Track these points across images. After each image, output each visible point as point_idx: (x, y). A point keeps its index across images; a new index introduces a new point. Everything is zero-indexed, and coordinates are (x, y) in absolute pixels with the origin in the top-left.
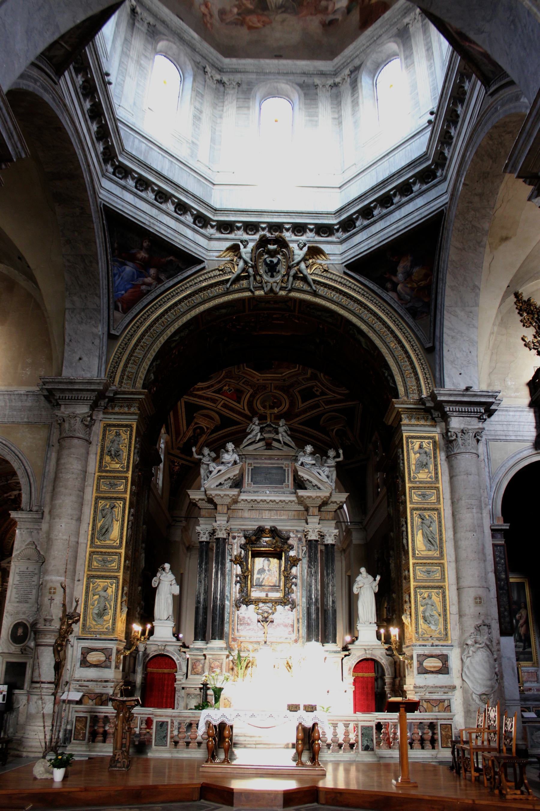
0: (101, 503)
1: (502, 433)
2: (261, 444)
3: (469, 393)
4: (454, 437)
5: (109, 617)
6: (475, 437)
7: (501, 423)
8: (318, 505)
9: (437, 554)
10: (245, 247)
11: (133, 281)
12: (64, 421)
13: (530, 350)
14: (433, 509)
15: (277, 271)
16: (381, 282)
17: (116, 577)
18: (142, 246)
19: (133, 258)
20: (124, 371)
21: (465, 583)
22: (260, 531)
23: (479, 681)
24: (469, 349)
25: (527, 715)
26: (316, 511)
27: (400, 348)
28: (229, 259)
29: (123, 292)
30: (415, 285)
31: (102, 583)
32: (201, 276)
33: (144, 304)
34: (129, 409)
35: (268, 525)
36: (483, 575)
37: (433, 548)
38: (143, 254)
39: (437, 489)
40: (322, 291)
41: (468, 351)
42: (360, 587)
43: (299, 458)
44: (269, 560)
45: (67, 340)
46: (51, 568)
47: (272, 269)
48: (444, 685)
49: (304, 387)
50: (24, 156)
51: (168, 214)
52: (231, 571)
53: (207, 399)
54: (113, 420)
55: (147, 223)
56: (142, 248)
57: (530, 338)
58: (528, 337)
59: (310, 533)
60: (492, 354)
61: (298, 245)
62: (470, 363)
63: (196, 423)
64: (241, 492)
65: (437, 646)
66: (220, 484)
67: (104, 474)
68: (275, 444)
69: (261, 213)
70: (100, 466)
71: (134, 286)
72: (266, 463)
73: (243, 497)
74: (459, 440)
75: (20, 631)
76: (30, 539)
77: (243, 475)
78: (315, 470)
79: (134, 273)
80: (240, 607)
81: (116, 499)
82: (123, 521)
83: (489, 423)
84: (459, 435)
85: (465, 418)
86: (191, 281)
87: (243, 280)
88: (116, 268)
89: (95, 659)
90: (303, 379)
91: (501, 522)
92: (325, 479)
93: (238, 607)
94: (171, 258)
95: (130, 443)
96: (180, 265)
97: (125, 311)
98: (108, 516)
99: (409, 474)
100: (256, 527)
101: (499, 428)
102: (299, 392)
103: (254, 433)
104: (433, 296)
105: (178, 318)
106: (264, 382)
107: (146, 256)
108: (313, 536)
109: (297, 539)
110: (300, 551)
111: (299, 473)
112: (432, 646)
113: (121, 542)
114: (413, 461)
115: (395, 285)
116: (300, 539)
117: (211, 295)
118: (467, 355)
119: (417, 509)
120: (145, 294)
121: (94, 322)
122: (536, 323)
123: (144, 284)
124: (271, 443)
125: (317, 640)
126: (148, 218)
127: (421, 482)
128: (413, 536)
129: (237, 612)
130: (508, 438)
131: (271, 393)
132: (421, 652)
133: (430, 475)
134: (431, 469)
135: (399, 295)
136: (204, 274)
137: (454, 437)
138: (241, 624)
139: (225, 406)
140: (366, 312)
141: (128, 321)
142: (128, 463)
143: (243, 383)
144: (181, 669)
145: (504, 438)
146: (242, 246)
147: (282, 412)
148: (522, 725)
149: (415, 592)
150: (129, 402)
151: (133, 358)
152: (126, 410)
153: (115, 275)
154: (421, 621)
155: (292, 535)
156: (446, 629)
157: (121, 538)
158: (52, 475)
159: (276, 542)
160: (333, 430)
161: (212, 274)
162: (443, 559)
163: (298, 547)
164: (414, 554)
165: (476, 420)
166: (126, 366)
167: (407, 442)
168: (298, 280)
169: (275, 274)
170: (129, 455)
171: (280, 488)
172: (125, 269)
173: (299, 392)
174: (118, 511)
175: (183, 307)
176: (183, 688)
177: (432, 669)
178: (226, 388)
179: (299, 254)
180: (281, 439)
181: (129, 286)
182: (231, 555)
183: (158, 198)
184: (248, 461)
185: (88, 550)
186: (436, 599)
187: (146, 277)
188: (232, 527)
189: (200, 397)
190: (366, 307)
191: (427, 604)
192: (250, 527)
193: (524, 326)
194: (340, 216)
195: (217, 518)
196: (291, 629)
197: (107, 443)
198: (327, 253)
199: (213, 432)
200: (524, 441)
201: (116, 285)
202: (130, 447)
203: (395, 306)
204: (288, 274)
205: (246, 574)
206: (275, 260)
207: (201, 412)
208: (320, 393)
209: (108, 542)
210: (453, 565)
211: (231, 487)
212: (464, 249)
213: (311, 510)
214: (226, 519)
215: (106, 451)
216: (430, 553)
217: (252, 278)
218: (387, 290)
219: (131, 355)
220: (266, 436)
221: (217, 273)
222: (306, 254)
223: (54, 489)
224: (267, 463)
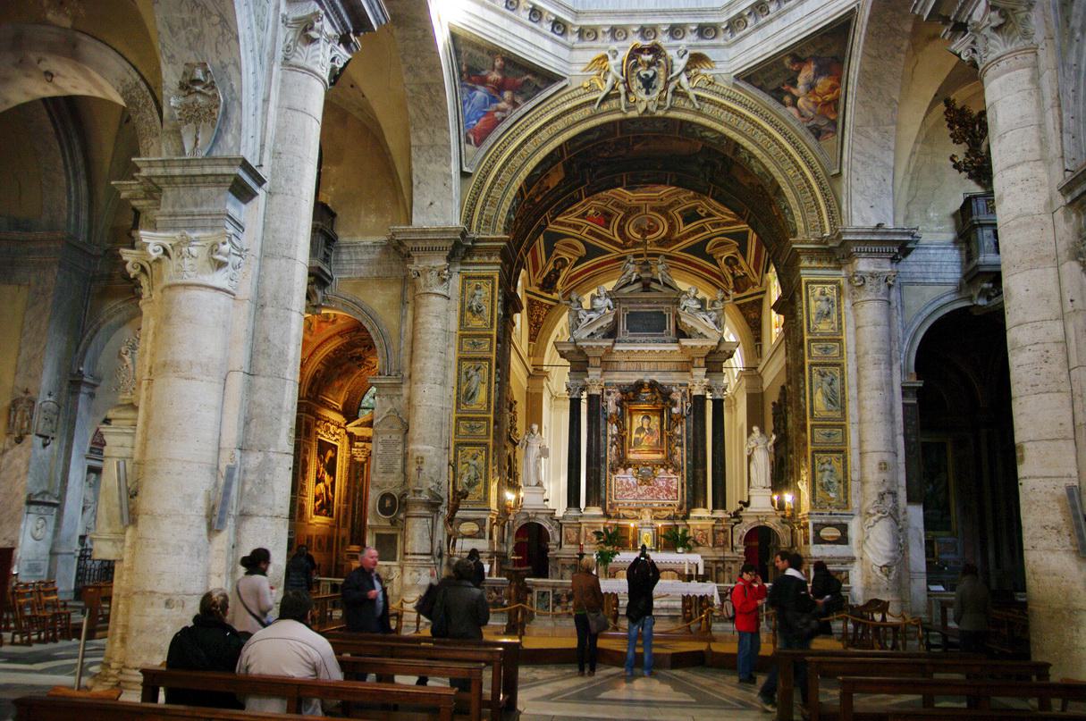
0: (466, 364)
1: (919, 275)
2: (637, 286)
3: (880, 230)
4: (862, 282)
5: (481, 486)
6: (886, 281)
8: (703, 356)
9: (838, 415)
10: (614, 57)
11: (485, 108)
12: (419, 275)
13: (960, 172)
14: (835, 365)
16: (778, 94)
17: (485, 444)
18: (494, 65)
19: (483, 81)
20: (481, 213)
21: (867, 447)
22: (639, 386)
23: (882, 552)
24: (882, 176)
25: (933, 588)
26: (702, 363)
27: (800, 177)
28: (595, 72)
29: (475, 122)
30: (820, 100)
31: (470, 450)
32: (563, 95)
33: (499, 134)
34: (489, 258)
35: (647, 379)
36: (890, 438)
37: (835, 408)
39: (840, 341)
40: (707, 109)
42: (753, 449)
43: (682, 301)
44: (648, 418)
45: (415, 182)
46: (416, 437)
47: (648, 83)
48: (842, 555)
49: (685, 207)
50: (384, 22)
51: (521, 24)
52: (606, 431)
53: (570, 226)
54: (472, 271)
55: (498, 37)
56: (493, 70)
57: (961, 158)
58: (959, 157)
59: (697, 387)
60: (912, 179)
61: (678, 53)
63: (557, 255)
64: (615, 342)
65: (835, 514)
66: (592, 334)
67: (466, 332)
68: (654, 285)
69: (632, 14)
70: (461, 325)
71: (486, 114)
72: (643, 308)
73: (618, 347)
74: (868, 286)
75: (388, 503)
76: (391, 406)
77: (617, 325)
78: (701, 316)
79: (486, 99)
80: (617, 470)
81: (481, 359)
82: (490, 383)
84: (868, 279)
86: (552, 103)
87: (612, 99)
88: (465, 95)
89: (467, 530)
90: (684, 198)
91: (914, 379)
92: (712, 326)
93: (614, 471)
94: (528, 77)
95: (493, 297)
96: (538, 84)
97: (478, 144)
98: (475, 378)
99: (809, 325)
100: (634, 381)
101: (916, 269)
102: (680, 213)
103: (629, 273)
104: (841, 113)
105: (539, 149)
106: (637, 202)
107: (500, 77)
108: (697, 391)
109: (679, 393)
110: (685, 408)
111: (682, 319)
112: (831, 514)
113: (489, 407)
114: (813, 310)
115: (795, 99)
116: (684, 395)
117: (576, 120)
118: (880, 183)
119: (816, 365)
120: (499, 122)
121: (444, 160)
122: (970, 137)
123: (498, 110)
124: (649, 284)
125: (705, 506)
126: (499, 32)
127: (822, 334)
128: (811, 394)
129: (613, 477)
130: (926, 281)
131: (645, 216)
132: (819, 521)
133: (832, 326)
135: (799, 111)
136: (566, 94)
137: (862, 282)
138: (619, 491)
139: (591, 233)
140: (760, 133)
141: (482, 155)
142: (492, 319)
143: (612, 205)
144: (554, 538)
145: (922, 281)
146: (610, 57)
147: (659, 238)
148: (926, 598)
149: (813, 456)
150: (489, 252)
151: (490, 199)
152: (486, 259)
154: (818, 489)
155: (674, 389)
156: (846, 497)
157: (489, 402)
158: (409, 335)
159: (656, 399)
160: (721, 258)
161: (576, 93)
162: (845, 421)
163: (682, 403)
164: (812, 414)
165: (888, 262)
166: (483, 207)
167: (807, 288)
168: (678, 96)
169: (650, 90)
170: (492, 310)
171: (660, 336)
172: (475, 94)
173: (680, 213)
174: (484, 372)
175: (544, 135)
176: (557, 558)
177: (830, 539)
178: (592, 211)
179: (680, 64)
180: (660, 279)
182: (606, 414)
183: (509, 4)
184: (623, 306)
185: (454, 416)
186: (837, 465)
188: (607, 381)
189: (561, 224)
190: (758, 126)
191: (824, 470)
192: (627, 381)
193: (954, 142)
194: (728, 13)
195: (590, 373)
196: (674, 495)
197: (467, 298)
198: (713, 60)
199: (577, 264)
200: (946, 284)
201: (467, 113)
202: (493, 301)
203: (794, 125)
204: (666, 88)
205: (624, 434)
206: (650, 73)
207: (561, 241)
208: (706, 214)
209: (474, 407)
210: (856, 427)
211: (604, 337)
212: (880, 56)
213: (696, 361)
214: (599, 373)
215: (467, 306)
216: (830, 414)
217: (623, 97)
218: (784, 104)
219: (488, 195)
220: (643, 276)
221: (583, 91)
222: (688, 63)
223: (412, 352)
224: (645, 308)
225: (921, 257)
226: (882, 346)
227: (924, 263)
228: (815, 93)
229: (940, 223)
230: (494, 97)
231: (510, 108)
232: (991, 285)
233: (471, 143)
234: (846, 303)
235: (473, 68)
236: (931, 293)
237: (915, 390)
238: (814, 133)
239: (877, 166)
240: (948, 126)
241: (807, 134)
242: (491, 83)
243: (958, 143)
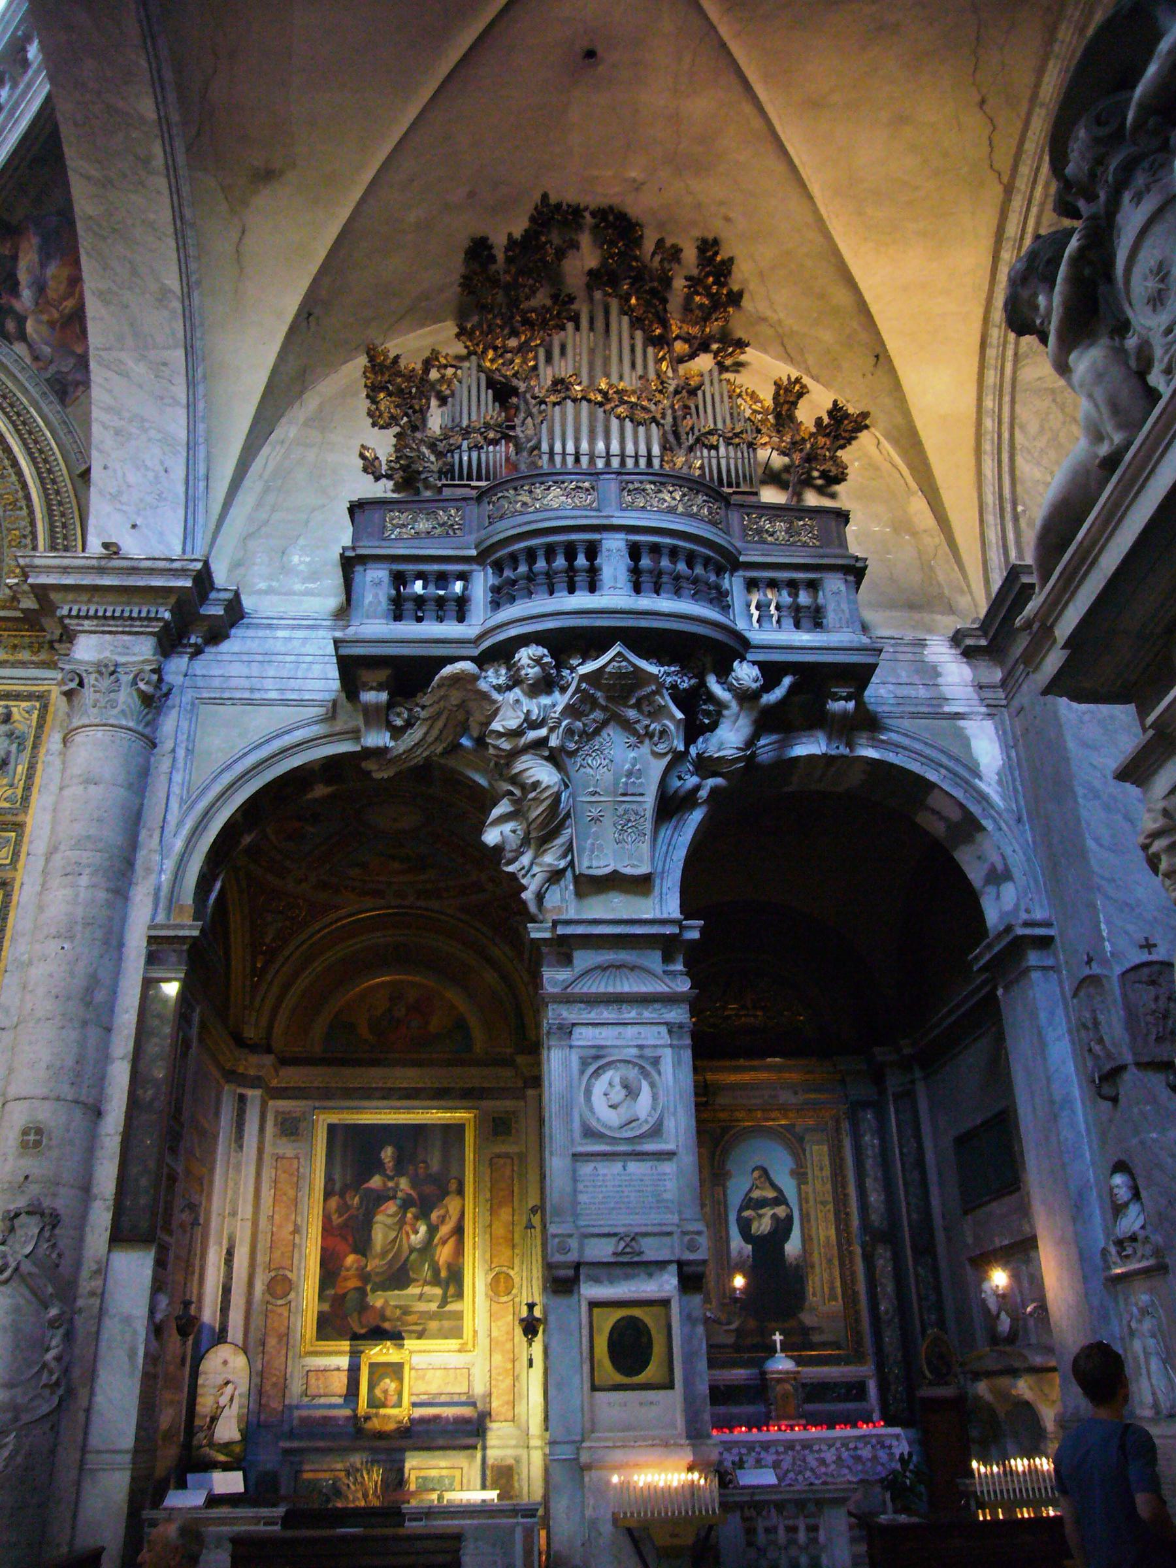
6: (134, 682)
7: (245, 658)
24: (162, 463)
39: (19, 827)
41: (161, 469)
62: (165, 499)
83: (211, 657)
84: (90, 680)
85: (120, 637)
101: (237, 669)
118: (157, 477)
130: (257, 695)
134: (17, 777)
225: (253, 645)
226: (92, 831)
227: (260, 658)
228: (48, 303)
229: (314, 576)
232: (383, 696)
234: (53, 741)
236: (262, 722)
237: (190, 941)
238: (56, 393)
239: (149, 440)
240: (368, 396)
241: (44, 393)
243: (382, 427)
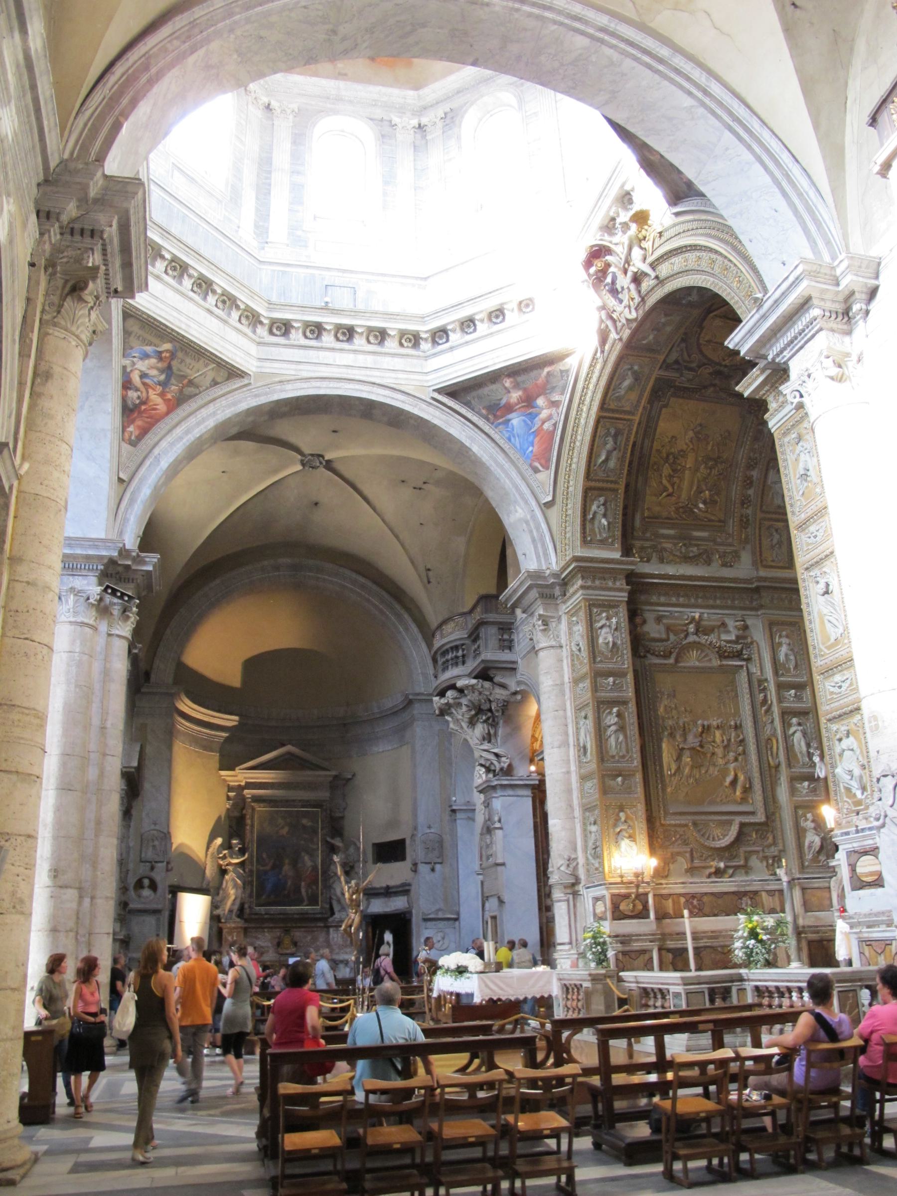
15: (620, 290)
18: (506, 388)
19: (509, 408)
38: (515, 396)
56: (509, 392)
65: (863, 830)
71: (536, 433)
79: (524, 421)
94: (546, 370)
97: (547, 468)
107: (520, 393)
112: (857, 832)
153: (509, 439)
177: (869, 879)
181: (532, 437)
183: (494, 320)
187: (540, 413)
230: (530, 414)
231: (553, 411)
233: (540, 471)
235: (490, 406)
242: (517, 404)
